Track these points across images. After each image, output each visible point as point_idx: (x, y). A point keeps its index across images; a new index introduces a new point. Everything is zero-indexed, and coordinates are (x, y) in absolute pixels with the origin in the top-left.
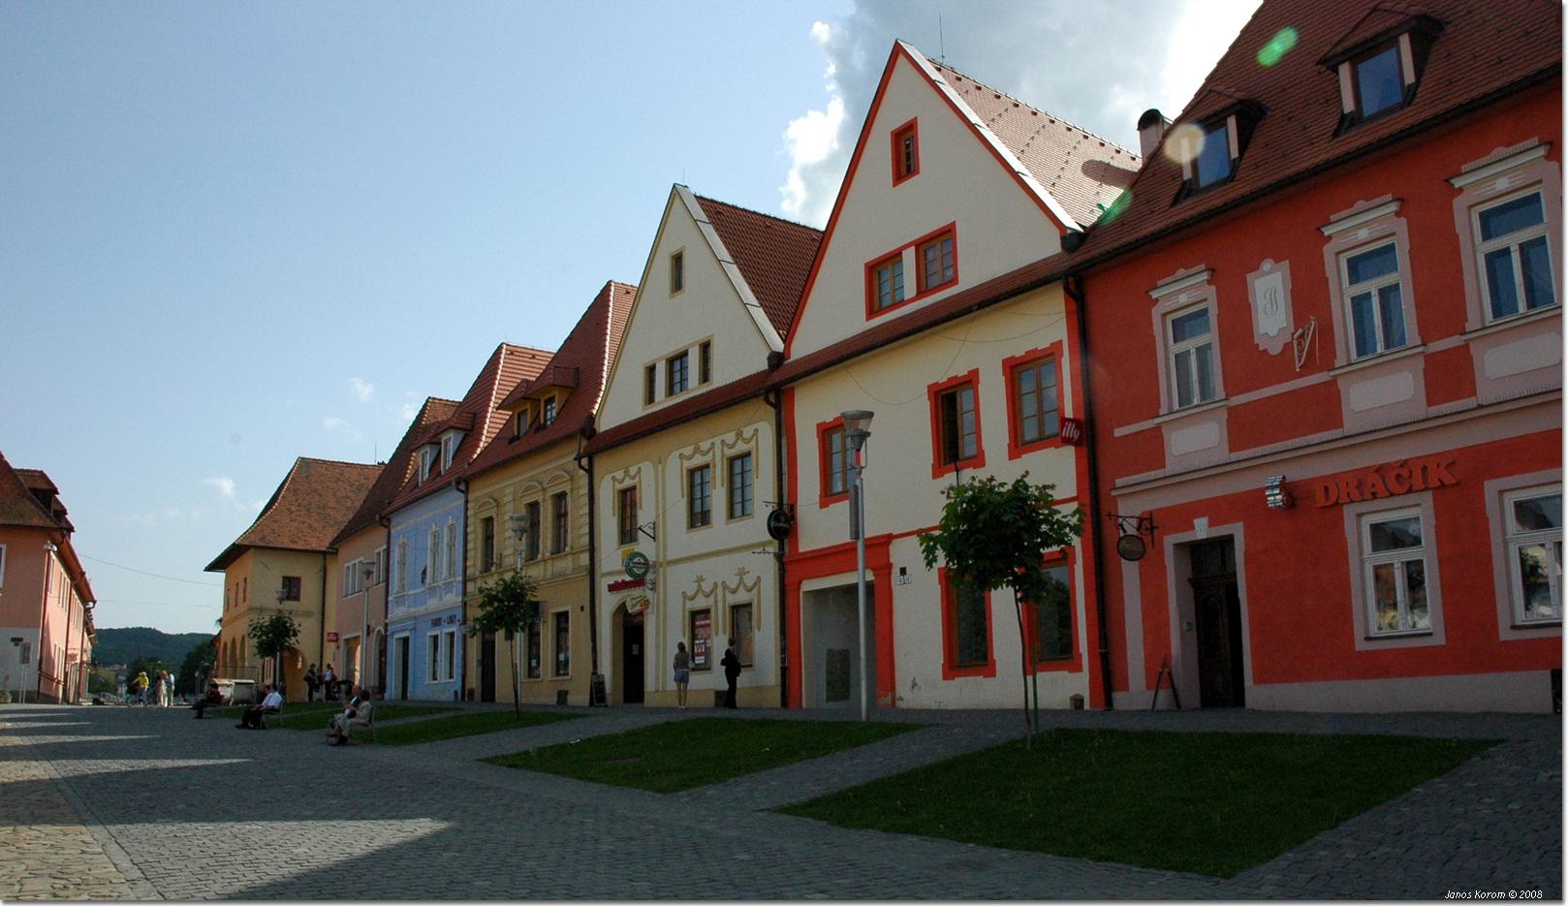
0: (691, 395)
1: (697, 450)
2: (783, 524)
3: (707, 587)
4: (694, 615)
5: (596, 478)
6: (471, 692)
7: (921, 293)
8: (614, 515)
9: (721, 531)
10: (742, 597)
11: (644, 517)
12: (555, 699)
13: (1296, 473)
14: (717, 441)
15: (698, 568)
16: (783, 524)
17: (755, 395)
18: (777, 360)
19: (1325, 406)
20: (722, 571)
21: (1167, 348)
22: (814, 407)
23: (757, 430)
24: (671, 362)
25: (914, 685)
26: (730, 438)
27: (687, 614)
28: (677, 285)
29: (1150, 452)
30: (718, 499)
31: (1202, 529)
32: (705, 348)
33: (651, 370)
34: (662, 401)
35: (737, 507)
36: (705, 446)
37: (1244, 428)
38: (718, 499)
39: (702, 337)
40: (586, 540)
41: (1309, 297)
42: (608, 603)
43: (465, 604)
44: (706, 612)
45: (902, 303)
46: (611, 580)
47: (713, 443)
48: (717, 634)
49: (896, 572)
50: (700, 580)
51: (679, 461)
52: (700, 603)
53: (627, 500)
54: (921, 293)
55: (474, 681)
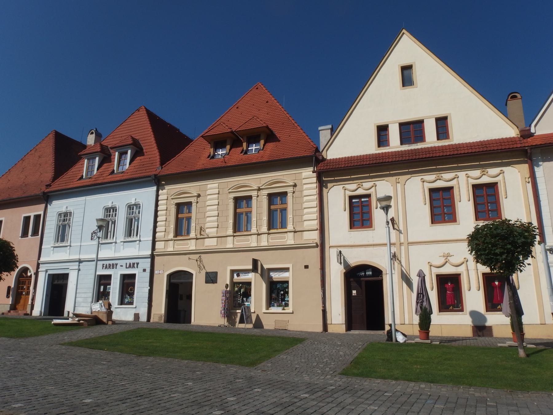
14: (462, 175)
33: (382, 130)
39: (441, 113)
40: (315, 224)
51: (421, 183)
52: (448, 270)
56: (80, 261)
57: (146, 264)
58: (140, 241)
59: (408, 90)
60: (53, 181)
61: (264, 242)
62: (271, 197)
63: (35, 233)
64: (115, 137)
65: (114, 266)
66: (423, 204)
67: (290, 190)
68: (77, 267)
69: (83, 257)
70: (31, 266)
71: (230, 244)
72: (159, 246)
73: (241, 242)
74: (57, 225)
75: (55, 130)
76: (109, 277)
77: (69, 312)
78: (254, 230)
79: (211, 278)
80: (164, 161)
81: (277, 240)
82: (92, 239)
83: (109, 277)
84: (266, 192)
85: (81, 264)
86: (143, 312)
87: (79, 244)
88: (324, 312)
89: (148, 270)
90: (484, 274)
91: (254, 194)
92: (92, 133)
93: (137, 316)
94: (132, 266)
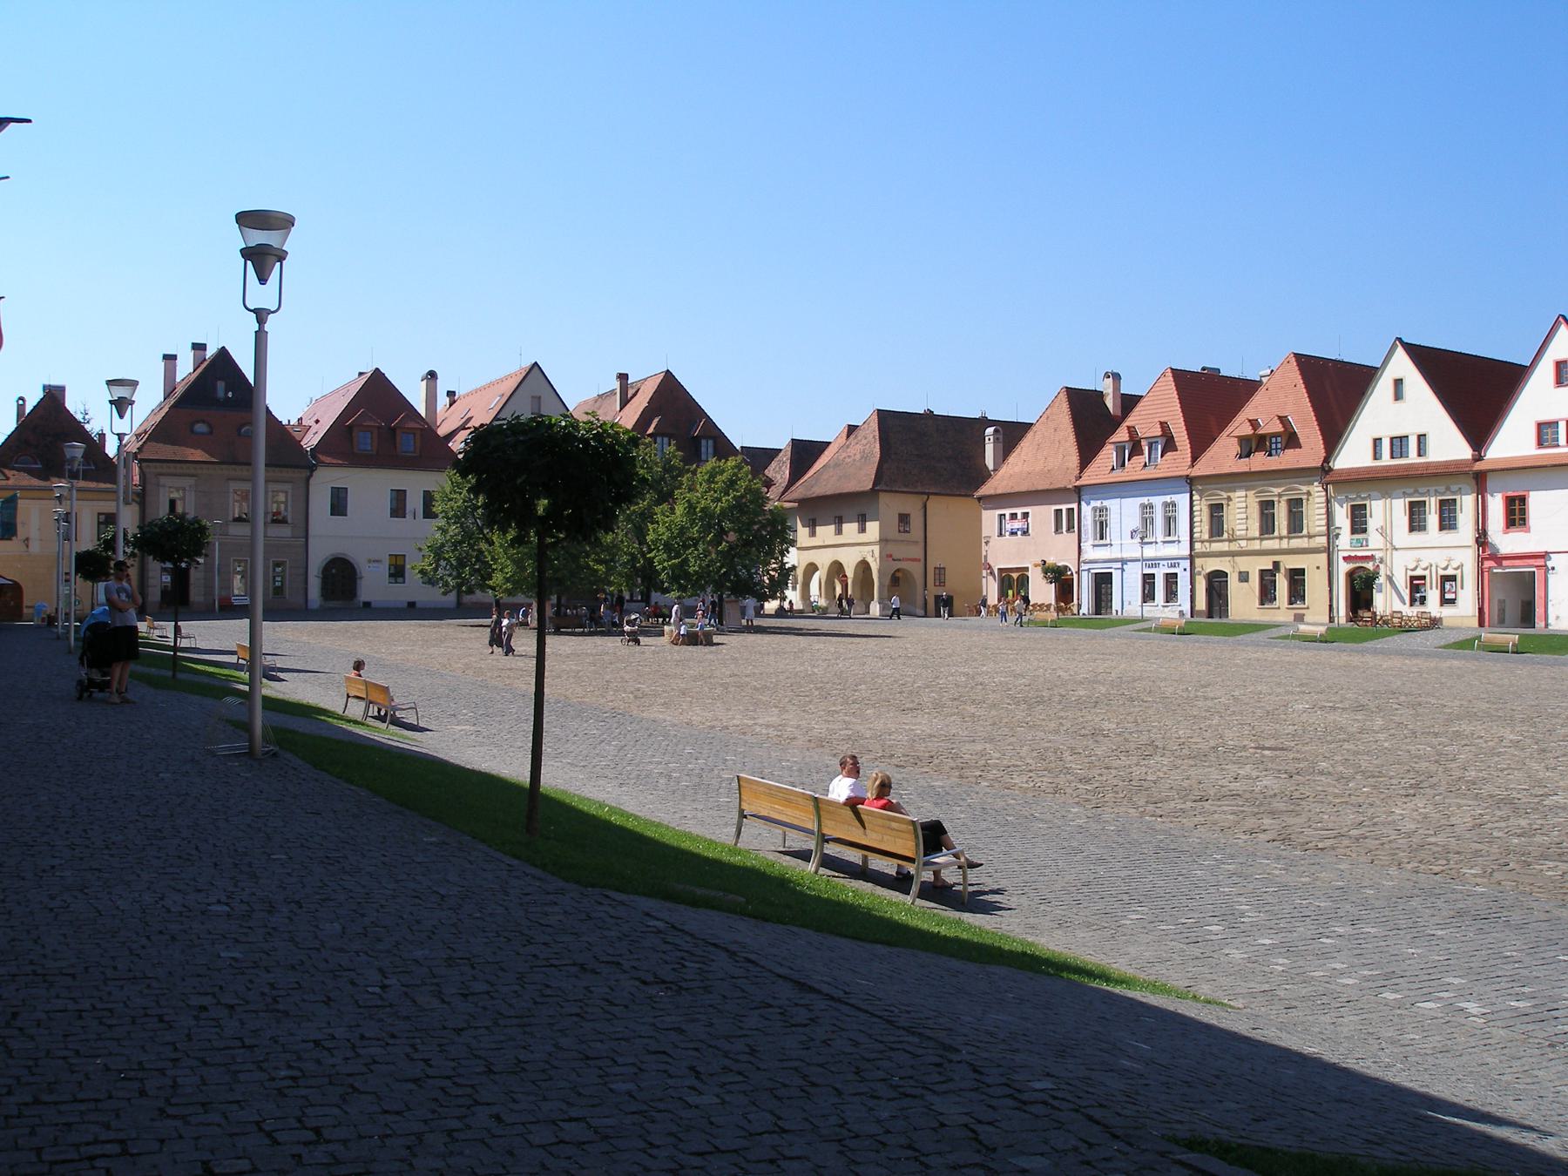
0: (1411, 462)
2: (1482, 539)
3: (1424, 565)
8: (1347, 517)
12: (1293, 618)
15: (1417, 554)
25: (1558, 617)
27: (1408, 579)
28: (1398, 395)
30: (1433, 519)
32: (1421, 438)
33: (1377, 442)
34: (1386, 460)
38: (1433, 519)
42: (1343, 568)
45: (1558, 446)
46: (1346, 554)
48: (1431, 588)
56: (1124, 561)
57: (1187, 564)
58: (1179, 542)
59: (1399, 404)
60: (1081, 471)
61: (1285, 544)
62: (1289, 501)
63: (1070, 528)
64: (1143, 413)
65: (1157, 566)
66: (1403, 514)
67: (1304, 497)
68: (1120, 566)
69: (1126, 555)
70: (1070, 563)
71: (1256, 545)
72: (1198, 546)
73: (1269, 544)
74: (1095, 522)
75: (1067, 388)
76: (1153, 576)
77: (1117, 611)
78: (1276, 534)
79: (1244, 577)
80: (1195, 458)
81: (1296, 543)
82: (1132, 538)
83: (1153, 576)
84: (1285, 498)
85: (1125, 566)
86: (1186, 607)
87: (1119, 542)
88: (1331, 606)
89: (1188, 569)
90: (1441, 576)
91: (1276, 499)
92: (1109, 377)
93: (1182, 613)
94: (1173, 566)
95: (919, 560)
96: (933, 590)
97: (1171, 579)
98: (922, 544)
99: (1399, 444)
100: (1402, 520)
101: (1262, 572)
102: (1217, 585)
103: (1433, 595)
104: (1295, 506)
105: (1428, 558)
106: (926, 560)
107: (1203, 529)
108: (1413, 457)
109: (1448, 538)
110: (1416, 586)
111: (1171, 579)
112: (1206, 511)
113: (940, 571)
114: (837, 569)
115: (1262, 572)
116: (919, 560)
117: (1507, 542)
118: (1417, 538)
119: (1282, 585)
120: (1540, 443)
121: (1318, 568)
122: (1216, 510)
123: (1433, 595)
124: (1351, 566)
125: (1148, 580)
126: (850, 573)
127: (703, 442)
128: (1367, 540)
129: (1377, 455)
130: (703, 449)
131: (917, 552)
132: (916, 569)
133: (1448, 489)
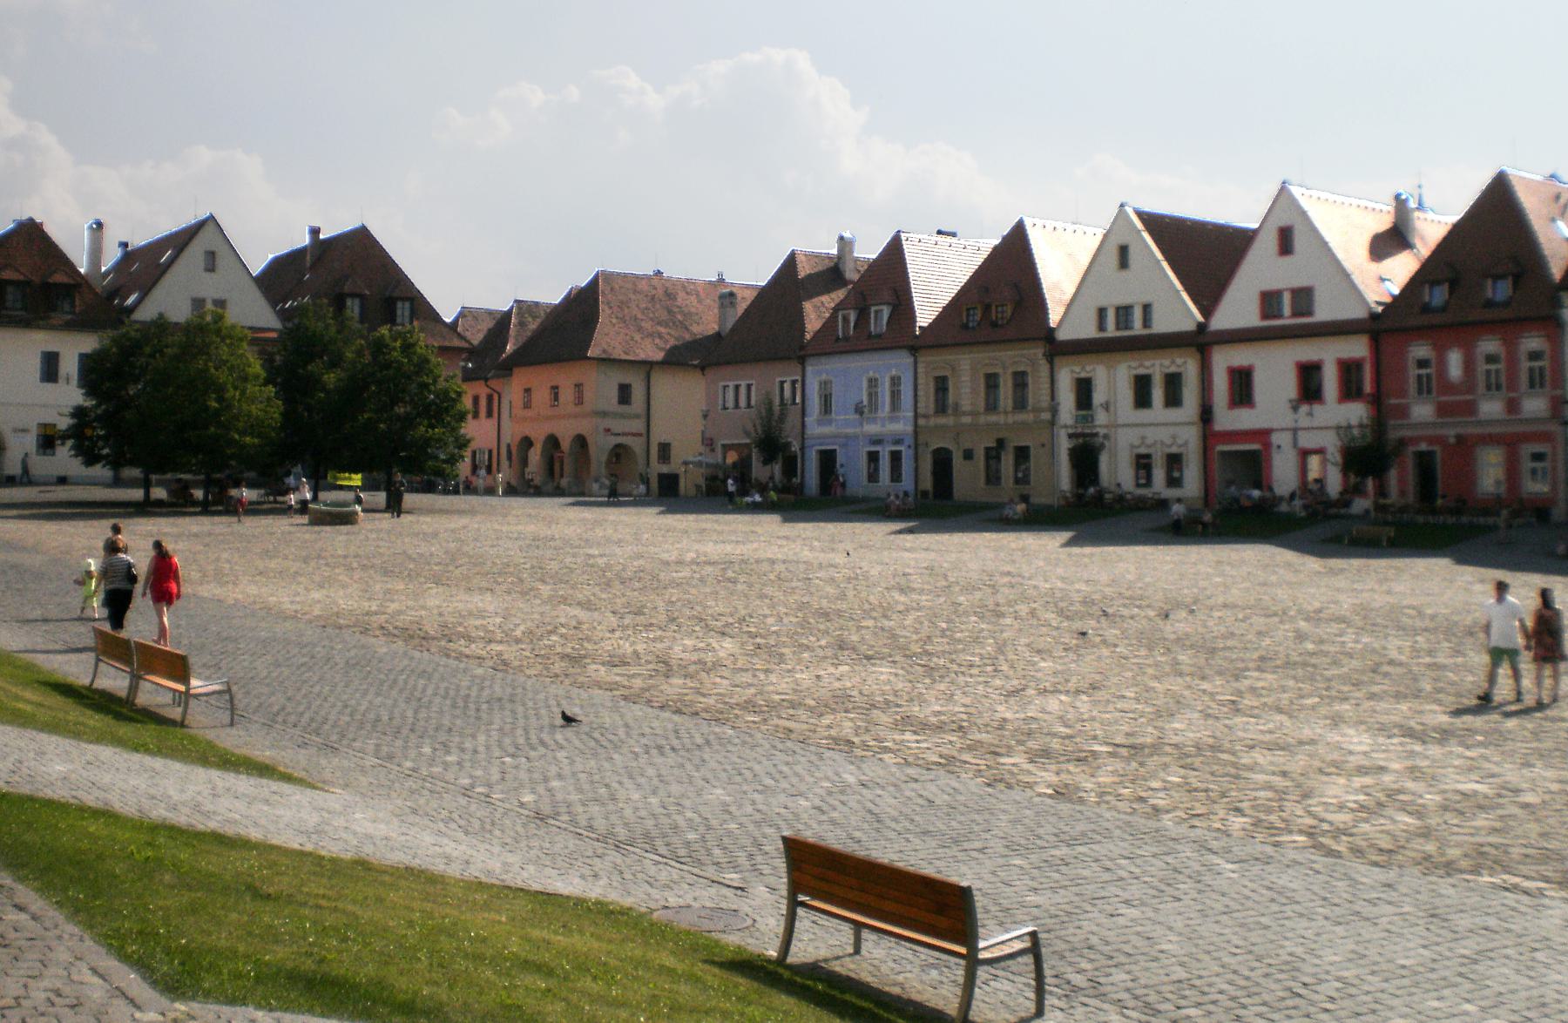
1: (1141, 365)
2: (1206, 414)
4: (1139, 457)
5: (1056, 369)
6: (925, 494)
7: (1295, 314)
9: (1158, 409)
10: (1174, 450)
11: (1098, 397)
13: (1460, 430)
14: (1158, 362)
16: (1206, 414)
17: (1189, 345)
18: (1202, 328)
19: (1470, 408)
20: (1163, 435)
21: (1413, 372)
22: (1224, 360)
23: (1189, 367)
24: (1118, 309)
26: (1167, 362)
29: (1403, 412)
30: (1158, 394)
31: (1423, 447)
32: (1147, 308)
33: (1102, 312)
34: (1111, 331)
35: (1173, 399)
36: (1147, 363)
37: (1443, 410)
38: (1158, 394)
41: (1469, 366)
42: (1064, 445)
43: (916, 433)
44: (1148, 456)
46: (1070, 431)
47: (1157, 366)
49: (1274, 447)
50: (1143, 438)
53: (1084, 389)
54: (1295, 314)
55: (927, 483)
59: (1124, 273)
79: (968, 455)
95: (640, 435)
96: (658, 468)
97: (896, 457)
98: (644, 420)
99: (1124, 312)
100: (1126, 394)
101: (988, 449)
102: (942, 463)
103: (1159, 475)
104: (1020, 381)
105: (1153, 435)
106: (648, 431)
107: (927, 401)
108: (1137, 328)
109: (1174, 414)
110: (1143, 464)
111: (896, 457)
112: (932, 385)
113: (665, 449)
114: (553, 442)
115: (988, 449)
116: (640, 435)
117: (1228, 419)
118: (1144, 415)
119: (1007, 462)
120: (1265, 316)
121: (1043, 445)
122: (941, 385)
123: (1159, 475)
124: (1074, 442)
125: (873, 457)
126: (566, 444)
127: (399, 304)
128: (1092, 416)
129: (1101, 326)
130: (399, 312)
131: (638, 425)
132: (637, 445)
133: (1173, 362)
